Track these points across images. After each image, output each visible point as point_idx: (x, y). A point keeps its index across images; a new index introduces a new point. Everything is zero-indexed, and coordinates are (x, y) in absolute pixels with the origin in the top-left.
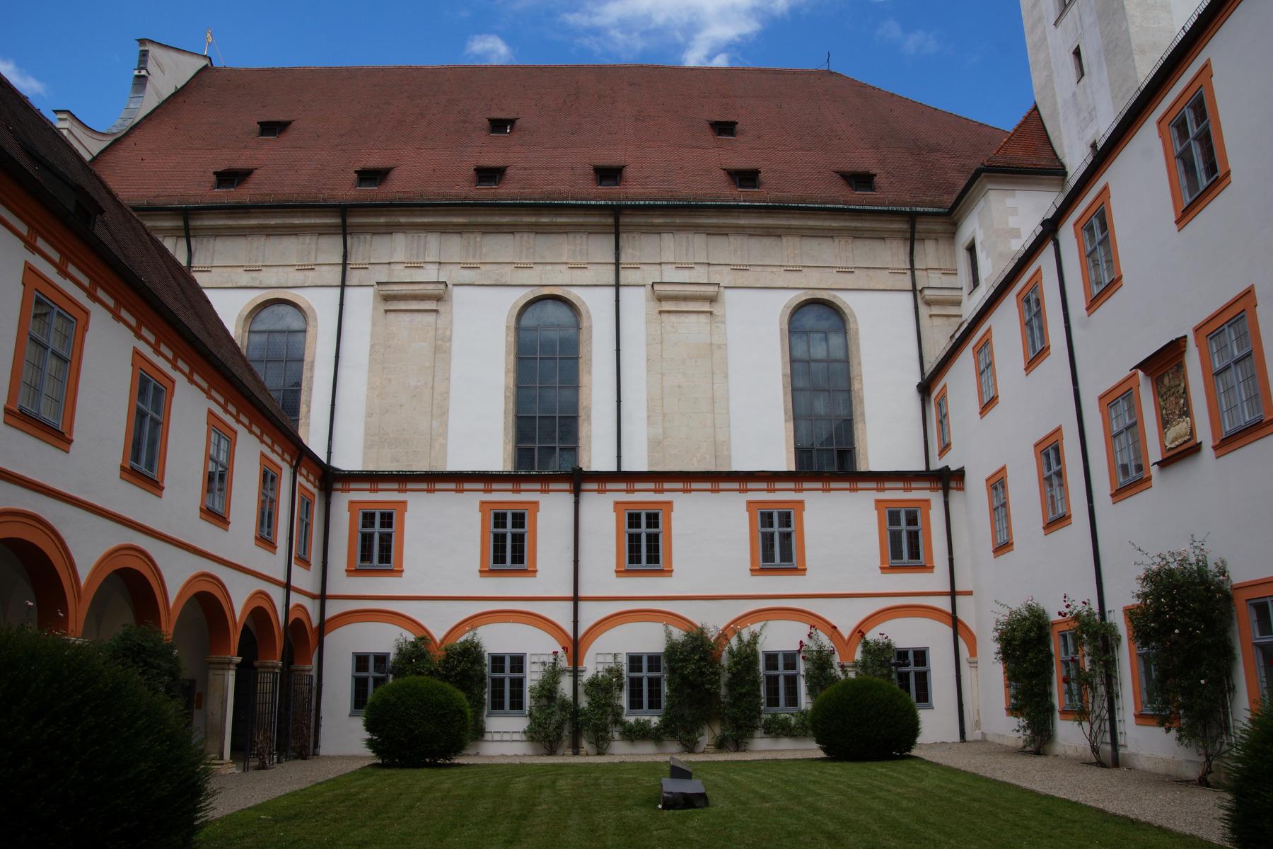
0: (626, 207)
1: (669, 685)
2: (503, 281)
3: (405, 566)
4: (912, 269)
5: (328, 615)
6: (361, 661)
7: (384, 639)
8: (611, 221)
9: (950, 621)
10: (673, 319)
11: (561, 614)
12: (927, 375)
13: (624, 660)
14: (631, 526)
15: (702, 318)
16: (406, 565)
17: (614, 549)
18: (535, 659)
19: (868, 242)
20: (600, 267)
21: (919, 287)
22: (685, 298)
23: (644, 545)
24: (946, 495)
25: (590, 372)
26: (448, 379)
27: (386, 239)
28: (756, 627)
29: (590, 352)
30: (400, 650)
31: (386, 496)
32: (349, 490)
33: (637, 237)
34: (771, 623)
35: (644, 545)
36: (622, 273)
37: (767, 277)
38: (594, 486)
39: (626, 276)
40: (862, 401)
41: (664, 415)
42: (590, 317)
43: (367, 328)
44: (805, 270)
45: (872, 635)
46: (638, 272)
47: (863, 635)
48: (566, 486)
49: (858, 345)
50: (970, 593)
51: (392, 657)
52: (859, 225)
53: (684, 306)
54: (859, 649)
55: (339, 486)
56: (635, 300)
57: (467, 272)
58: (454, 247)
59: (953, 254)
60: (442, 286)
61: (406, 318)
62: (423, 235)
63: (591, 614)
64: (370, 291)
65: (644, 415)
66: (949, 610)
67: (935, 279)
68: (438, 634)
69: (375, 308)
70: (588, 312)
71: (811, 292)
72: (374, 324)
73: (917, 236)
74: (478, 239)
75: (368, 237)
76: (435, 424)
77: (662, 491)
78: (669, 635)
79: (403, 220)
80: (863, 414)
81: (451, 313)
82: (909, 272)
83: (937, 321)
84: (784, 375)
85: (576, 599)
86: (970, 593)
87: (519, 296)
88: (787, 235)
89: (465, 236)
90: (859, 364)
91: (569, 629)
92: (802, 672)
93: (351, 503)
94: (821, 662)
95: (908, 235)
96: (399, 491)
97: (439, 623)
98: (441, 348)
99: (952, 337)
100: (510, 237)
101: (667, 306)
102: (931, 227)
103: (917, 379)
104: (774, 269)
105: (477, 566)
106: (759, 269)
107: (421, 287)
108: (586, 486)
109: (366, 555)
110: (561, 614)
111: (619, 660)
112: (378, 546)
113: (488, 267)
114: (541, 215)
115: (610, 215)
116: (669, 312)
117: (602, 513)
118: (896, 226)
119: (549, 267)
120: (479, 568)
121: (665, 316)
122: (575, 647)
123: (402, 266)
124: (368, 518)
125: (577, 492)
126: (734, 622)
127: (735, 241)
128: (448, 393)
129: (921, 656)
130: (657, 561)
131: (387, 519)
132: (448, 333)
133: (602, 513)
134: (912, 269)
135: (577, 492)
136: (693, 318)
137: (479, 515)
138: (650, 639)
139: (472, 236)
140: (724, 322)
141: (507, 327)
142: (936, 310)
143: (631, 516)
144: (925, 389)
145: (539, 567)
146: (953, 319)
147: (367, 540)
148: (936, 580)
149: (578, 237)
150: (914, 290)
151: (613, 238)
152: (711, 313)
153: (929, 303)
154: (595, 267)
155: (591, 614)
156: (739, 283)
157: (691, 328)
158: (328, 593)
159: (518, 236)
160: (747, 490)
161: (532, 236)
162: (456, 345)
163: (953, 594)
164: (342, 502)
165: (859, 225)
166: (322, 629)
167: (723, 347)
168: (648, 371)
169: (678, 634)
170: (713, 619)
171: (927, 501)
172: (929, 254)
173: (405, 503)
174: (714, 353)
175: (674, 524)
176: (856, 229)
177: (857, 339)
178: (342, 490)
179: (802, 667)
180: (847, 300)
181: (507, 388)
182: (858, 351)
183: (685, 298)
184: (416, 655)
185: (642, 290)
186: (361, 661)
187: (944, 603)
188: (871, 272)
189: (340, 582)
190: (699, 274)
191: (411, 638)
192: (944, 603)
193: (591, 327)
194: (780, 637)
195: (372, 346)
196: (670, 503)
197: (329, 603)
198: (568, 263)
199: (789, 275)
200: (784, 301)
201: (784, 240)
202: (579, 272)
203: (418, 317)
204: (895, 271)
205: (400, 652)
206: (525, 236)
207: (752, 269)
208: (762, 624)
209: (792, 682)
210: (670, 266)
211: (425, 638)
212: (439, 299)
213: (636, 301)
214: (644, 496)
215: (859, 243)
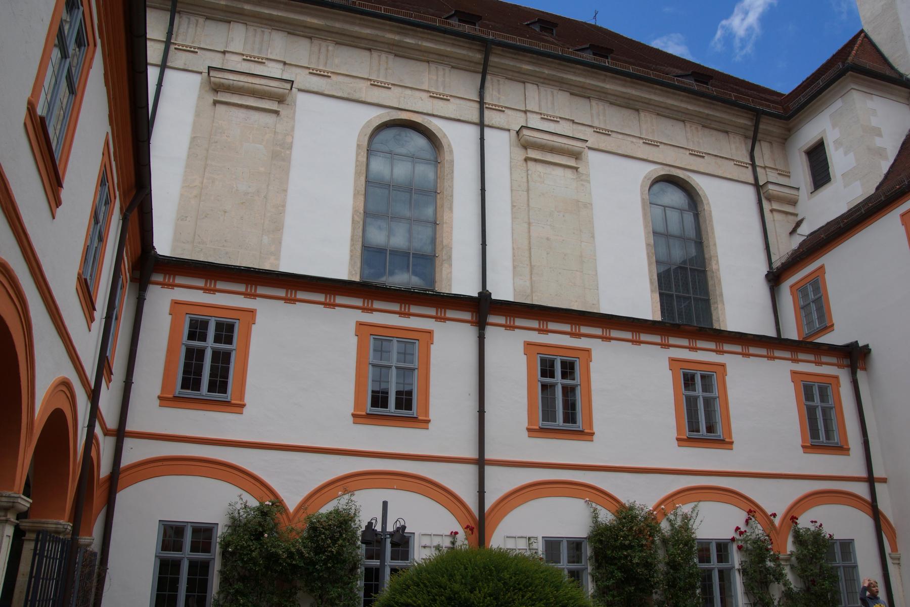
0: (499, 44)
1: (595, 580)
2: (356, 96)
3: (248, 399)
4: (754, 166)
5: (125, 462)
6: (172, 534)
7: (211, 504)
8: (478, 57)
9: (869, 510)
10: (540, 168)
11: (461, 481)
12: (777, 264)
13: (540, 547)
14: (544, 374)
15: (569, 173)
16: (249, 398)
17: (525, 401)
18: (426, 541)
19: (715, 133)
20: (462, 102)
21: (761, 183)
22: (553, 150)
23: (560, 400)
24: (854, 374)
25: (451, 209)
26: (286, 191)
27: (223, 27)
28: (686, 509)
29: (451, 187)
30: (233, 518)
31: (227, 299)
32: (173, 286)
33: (502, 81)
34: (701, 504)
35: (560, 400)
36: (487, 113)
37: (627, 146)
38: (501, 320)
39: (490, 117)
40: (720, 281)
41: (532, 267)
42: (451, 152)
43: (188, 117)
44: (662, 146)
45: (804, 522)
46: (501, 114)
47: (794, 519)
48: (467, 316)
49: (712, 229)
50: (884, 480)
51: (221, 531)
52: (711, 113)
53: (549, 157)
54: (790, 540)
55: (159, 278)
56: (499, 144)
57: (315, 79)
58: (301, 51)
59: (786, 157)
60: (288, 86)
61: (241, 113)
62: (267, 31)
63: (500, 484)
64: (197, 79)
65: (509, 264)
66: (867, 497)
67: (773, 177)
68: (292, 502)
69: (200, 97)
70: (449, 146)
71: (667, 168)
72: (198, 114)
73: (760, 136)
74: (330, 48)
75: (201, 20)
76: (266, 239)
77: (579, 335)
78: (596, 517)
79: (247, 7)
80: (721, 295)
81: (293, 118)
82: (750, 167)
83: (777, 216)
84: (648, 245)
85: (481, 462)
86: (884, 480)
87: (376, 116)
88: (645, 110)
89: (316, 42)
90: (715, 245)
91: (471, 501)
92: (737, 566)
93: (175, 303)
94: (758, 552)
95: (751, 134)
96: (246, 295)
97: (294, 484)
98: (280, 154)
99: (793, 232)
100: (366, 54)
101: (533, 154)
102: (770, 128)
103: (764, 269)
104: (634, 140)
105: (350, 408)
106: (620, 136)
107: (263, 81)
108: (492, 319)
109: (191, 380)
110: (461, 481)
111: (535, 546)
112: (208, 369)
113: (340, 78)
114: (406, 35)
115: (479, 51)
116: (536, 160)
117: (510, 353)
118: (742, 121)
119: (408, 92)
120: (351, 410)
121: (530, 164)
122: (479, 526)
123: (239, 58)
124: (197, 330)
125: (481, 325)
126: (662, 502)
127: (597, 107)
128: (284, 206)
129: (847, 546)
130: (574, 421)
131: (225, 332)
132: (289, 139)
133: (510, 353)
134: (754, 166)
135: (481, 325)
136: (559, 171)
137: (354, 340)
138: (570, 519)
139: (324, 44)
140: (589, 182)
141: (358, 146)
142: (775, 206)
143: (543, 361)
144: (775, 278)
145: (432, 416)
146: (791, 218)
147: (194, 357)
148: (852, 464)
149: (440, 67)
150: (757, 186)
151: (479, 78)
152: (576, 169)
153: (770, 199)
154: (458, 101)
155: (500, 484)
156: (602, 146)
157: (554, 180)
158: (129, 427)
159: (375, 55)
160: (669, 346)
161: (391, 57)
162: (297, 155)
163: (871, 480)
164: (161, 301)
165: (711, 113)
166: (114, 483)
167: (588, 206)
168: (514, 218)
169: (606, 517)
170: (642, 495)
171: (837, 377)
172: (765, 155)
173: (252, 312)
174: (580, 208)
175: (594, 376)
176: (707, 117)
177: (711, 220)
178: (163, 285)
179: (736, 559)
180: (700, 183)
181: (355, 211)
182: (713, 233)
183: (553, 150)
184: (259, 527)
185: (506, 134)
186: (172, 534)
187: (861, 490)
188: (719, 160)
189: (147, 413)
190: (564, 128)
191: (254, 503)
192: (861, 490)
193: (452, 161)
194: (714, 523)
195: (193, 139)
196: (588, 351)
197: (128, 443)
198: (434, 92)
199: (647, 147)
200: (644, 171)
201: (642, 114)
202: (441, 103)
203: (255, 116)
204: (739, 164)
205: (235, 524)
206: (384, 56)
207: (614, 135)
208: (692, 505)
209: (725, 576)
210: (535, 116)
211: (278, 503)
212: (281, 99)
213: (499, 144)
214: (559, 338)
215: (707, 131)
